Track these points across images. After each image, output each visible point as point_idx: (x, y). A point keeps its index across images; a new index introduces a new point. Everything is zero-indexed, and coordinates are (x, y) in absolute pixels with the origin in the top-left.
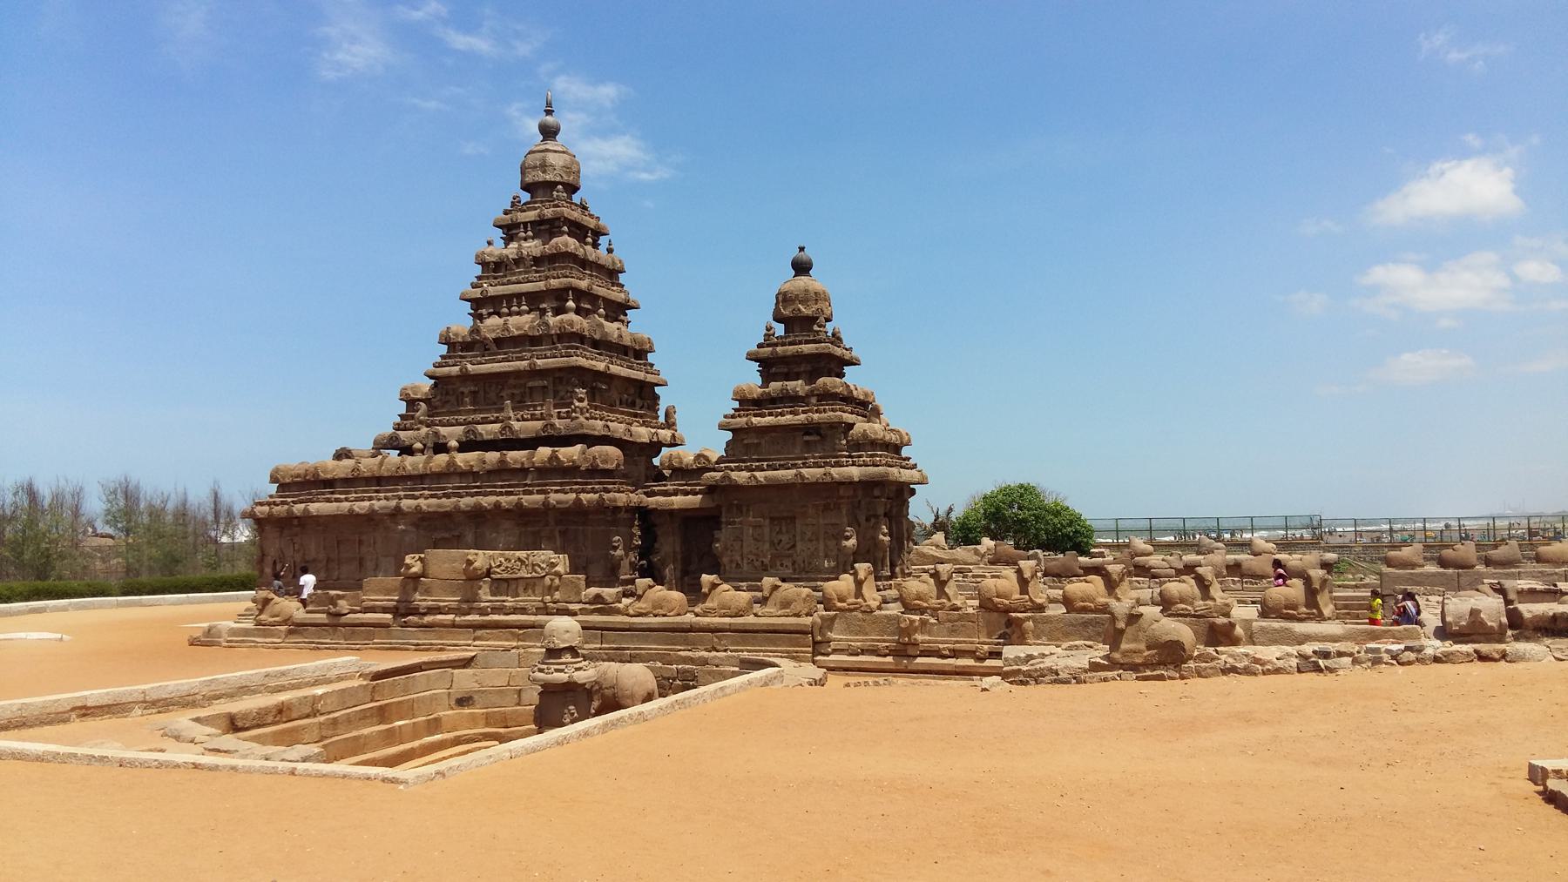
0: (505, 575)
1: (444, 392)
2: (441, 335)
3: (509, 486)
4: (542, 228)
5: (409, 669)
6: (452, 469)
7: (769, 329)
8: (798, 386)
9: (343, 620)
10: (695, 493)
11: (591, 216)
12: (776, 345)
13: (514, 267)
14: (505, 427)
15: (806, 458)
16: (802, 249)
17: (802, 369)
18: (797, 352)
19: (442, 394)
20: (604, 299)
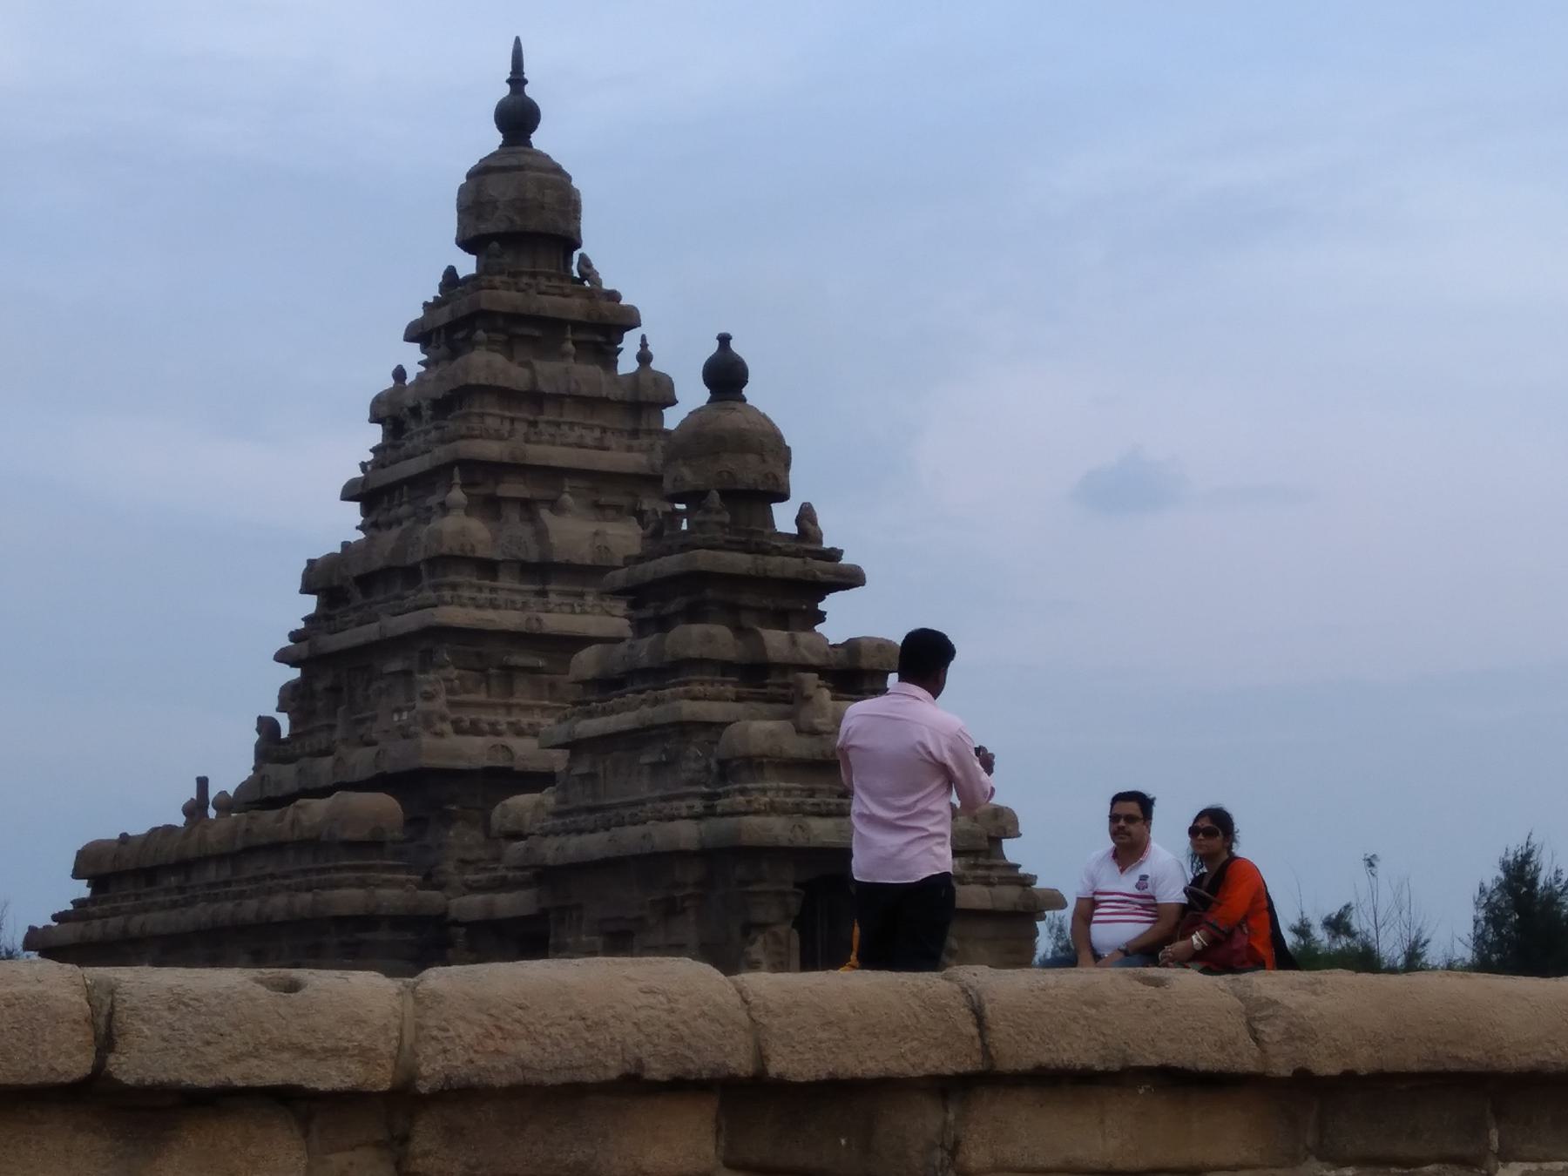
4: (460, 335)
15: (642, 803)
16: (724, 340)
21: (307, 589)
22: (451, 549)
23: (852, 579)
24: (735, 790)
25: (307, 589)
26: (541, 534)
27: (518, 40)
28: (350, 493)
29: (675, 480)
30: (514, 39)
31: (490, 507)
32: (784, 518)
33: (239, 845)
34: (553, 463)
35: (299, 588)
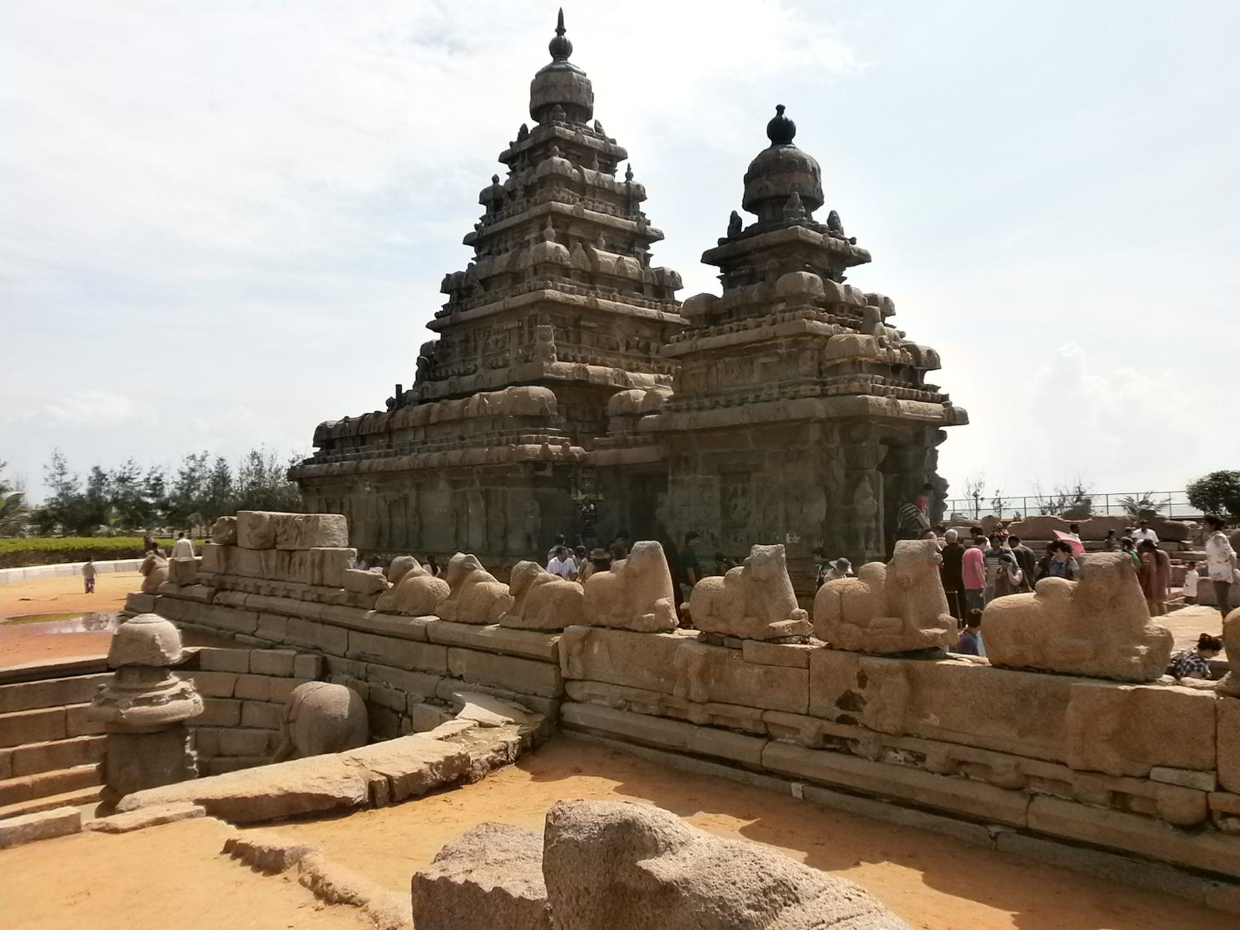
0: (287, 547)
1: (445, 345)
2: (443, 284)
3: (447, 440)
4: (538, 153)
5: (66, 670)
6: (405, 425)
7: (735, 220)
8: (755, 292)
9: (186, 592)
10: (645, 443)
11: (603, 137)
12: (737, 239)
13: (510, 201)
14: (478, 377)
16: (780, 109)
17: (767, 268)
18: (758, 243)
19: (442, 347)
20: (605, 227)
21: (445, 289)
22: (550, 258)
23: (863, 258)
24: (845, 379)
25: (445, 289)
26: (593, 257)
27: (561, 10)
28: (468, 241)
29: (761, 189)
30: (559, 10)
31: (563, 239)
32: (820, 216)
33: (433, 419)
34: (595, 220)
35: (440, 289)
